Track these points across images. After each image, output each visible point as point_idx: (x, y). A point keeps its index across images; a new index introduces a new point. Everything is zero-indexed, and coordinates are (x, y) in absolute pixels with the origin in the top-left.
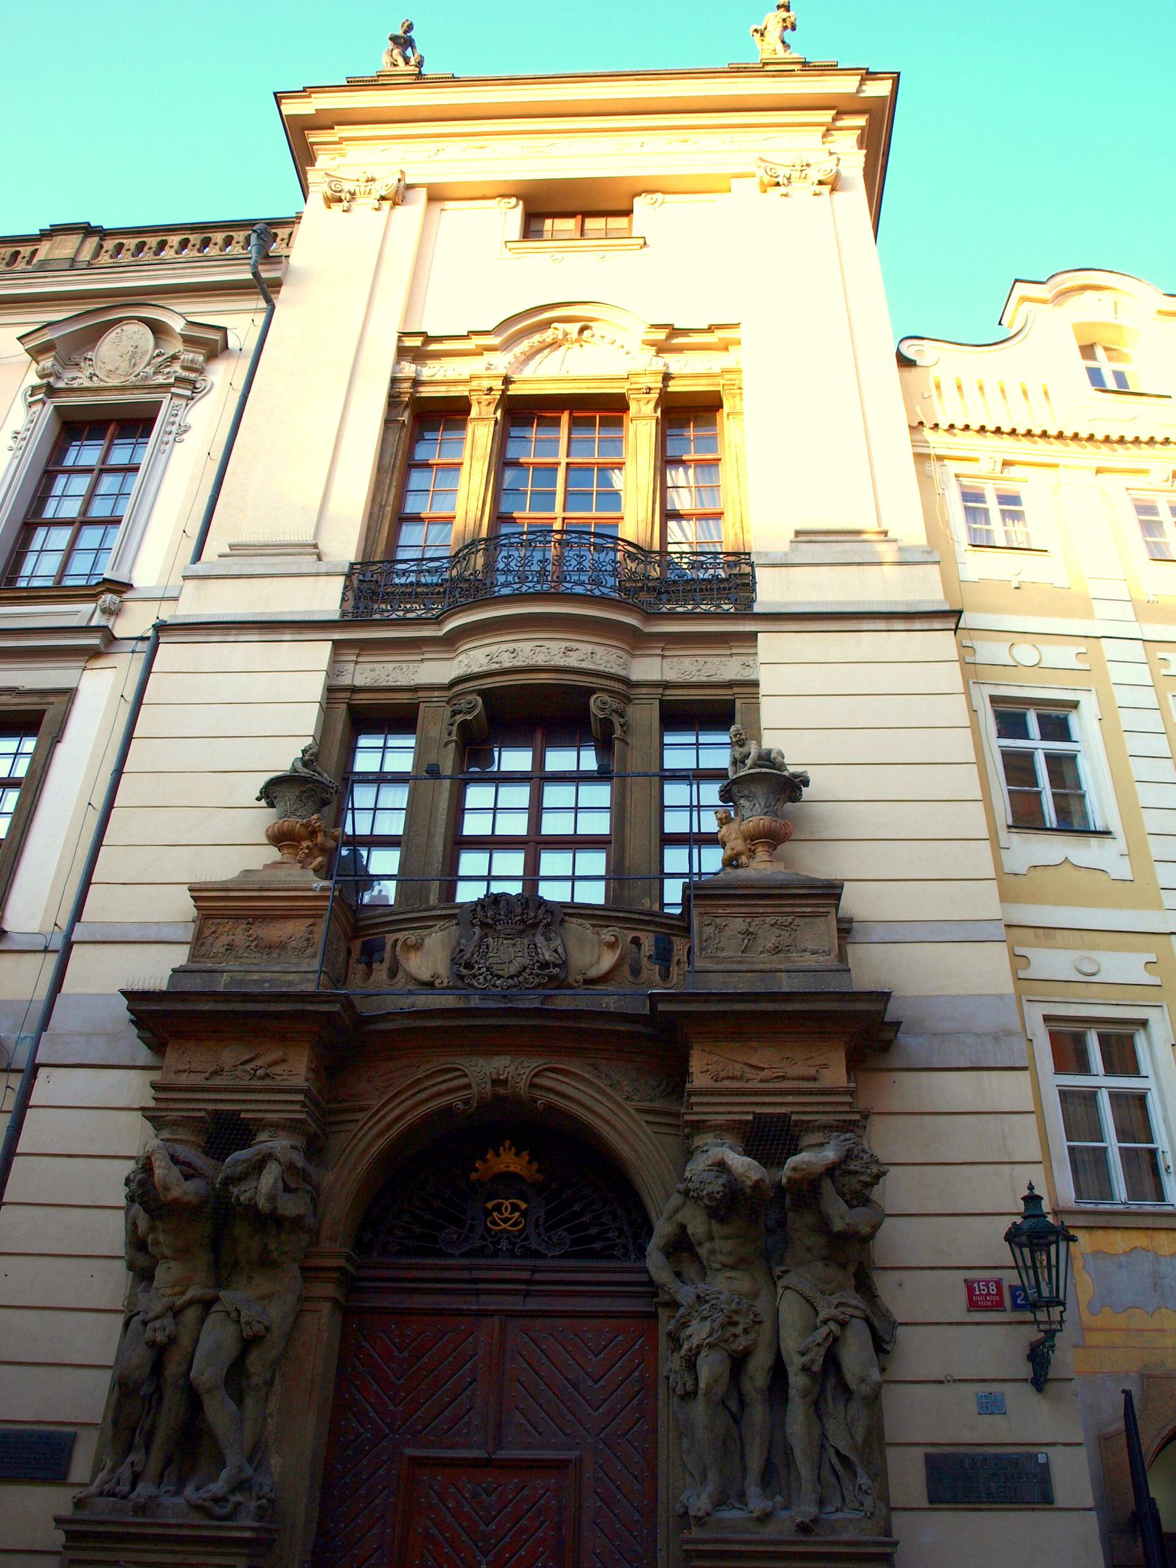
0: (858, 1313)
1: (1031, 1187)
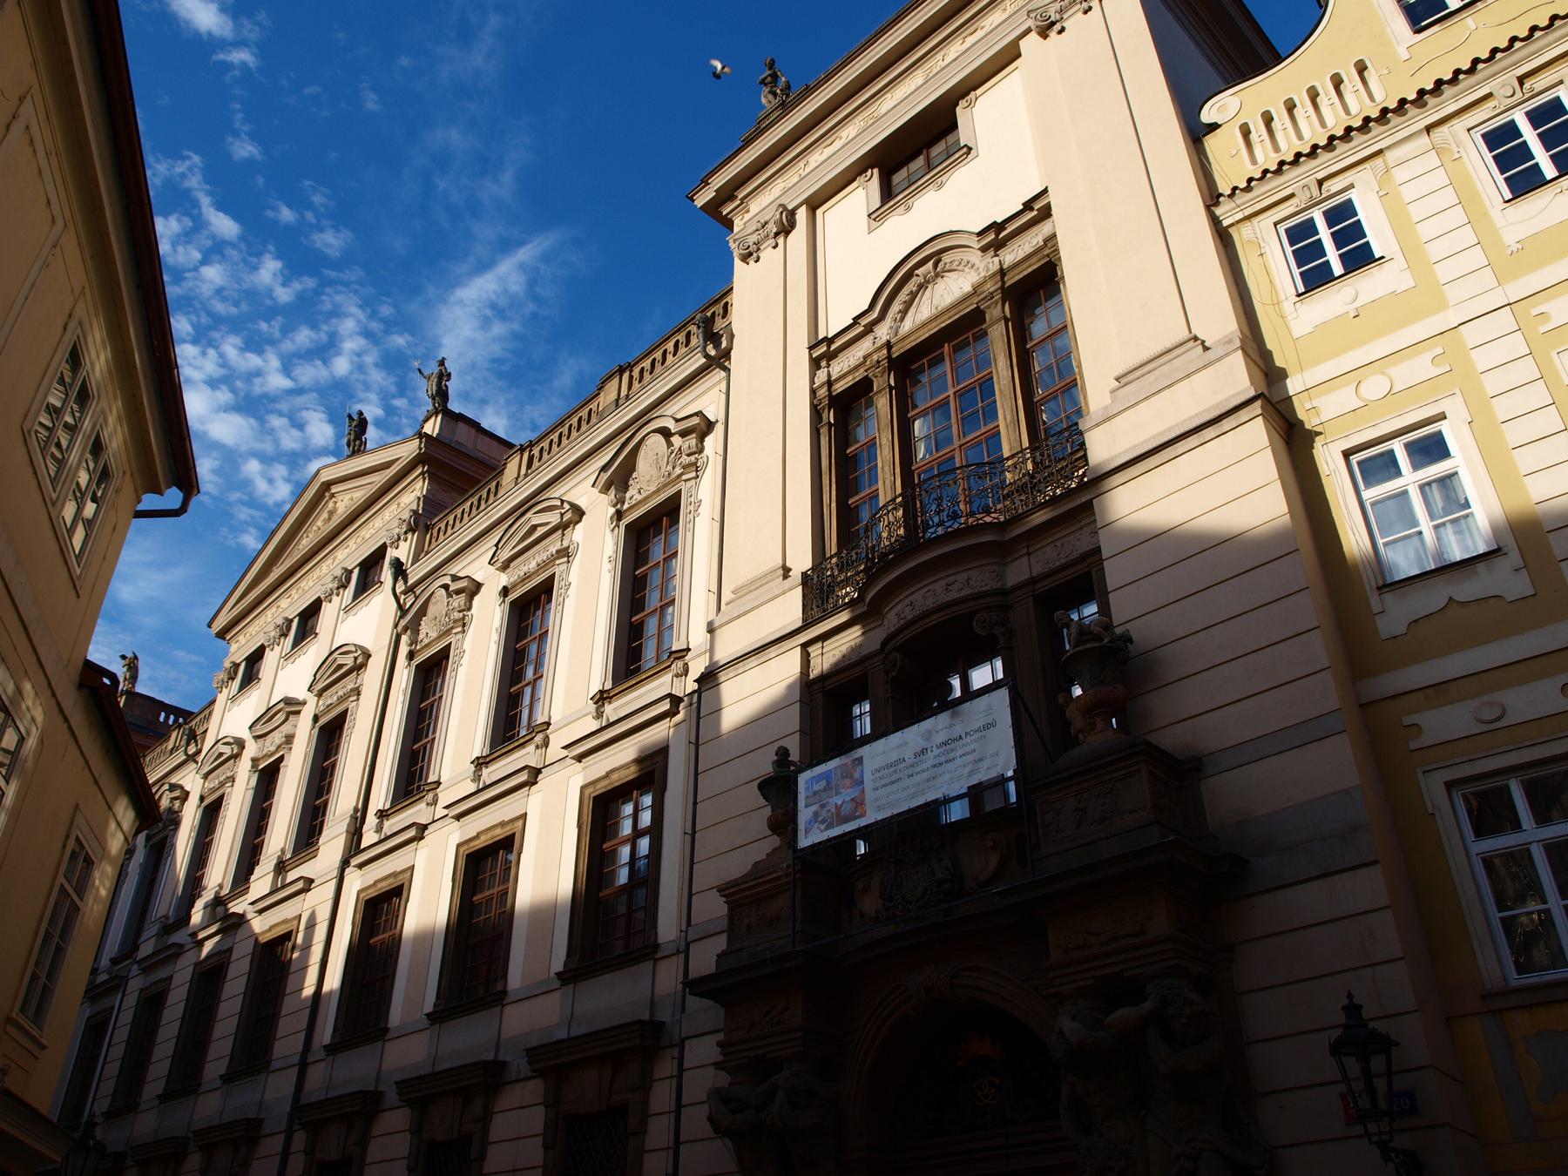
1: (1350, 996)
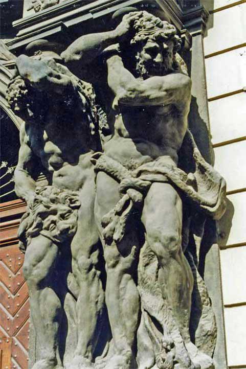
0: (160, 177)
